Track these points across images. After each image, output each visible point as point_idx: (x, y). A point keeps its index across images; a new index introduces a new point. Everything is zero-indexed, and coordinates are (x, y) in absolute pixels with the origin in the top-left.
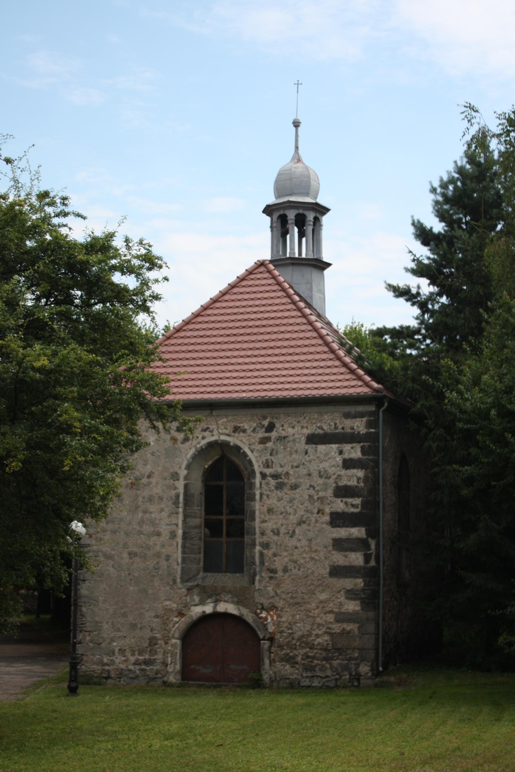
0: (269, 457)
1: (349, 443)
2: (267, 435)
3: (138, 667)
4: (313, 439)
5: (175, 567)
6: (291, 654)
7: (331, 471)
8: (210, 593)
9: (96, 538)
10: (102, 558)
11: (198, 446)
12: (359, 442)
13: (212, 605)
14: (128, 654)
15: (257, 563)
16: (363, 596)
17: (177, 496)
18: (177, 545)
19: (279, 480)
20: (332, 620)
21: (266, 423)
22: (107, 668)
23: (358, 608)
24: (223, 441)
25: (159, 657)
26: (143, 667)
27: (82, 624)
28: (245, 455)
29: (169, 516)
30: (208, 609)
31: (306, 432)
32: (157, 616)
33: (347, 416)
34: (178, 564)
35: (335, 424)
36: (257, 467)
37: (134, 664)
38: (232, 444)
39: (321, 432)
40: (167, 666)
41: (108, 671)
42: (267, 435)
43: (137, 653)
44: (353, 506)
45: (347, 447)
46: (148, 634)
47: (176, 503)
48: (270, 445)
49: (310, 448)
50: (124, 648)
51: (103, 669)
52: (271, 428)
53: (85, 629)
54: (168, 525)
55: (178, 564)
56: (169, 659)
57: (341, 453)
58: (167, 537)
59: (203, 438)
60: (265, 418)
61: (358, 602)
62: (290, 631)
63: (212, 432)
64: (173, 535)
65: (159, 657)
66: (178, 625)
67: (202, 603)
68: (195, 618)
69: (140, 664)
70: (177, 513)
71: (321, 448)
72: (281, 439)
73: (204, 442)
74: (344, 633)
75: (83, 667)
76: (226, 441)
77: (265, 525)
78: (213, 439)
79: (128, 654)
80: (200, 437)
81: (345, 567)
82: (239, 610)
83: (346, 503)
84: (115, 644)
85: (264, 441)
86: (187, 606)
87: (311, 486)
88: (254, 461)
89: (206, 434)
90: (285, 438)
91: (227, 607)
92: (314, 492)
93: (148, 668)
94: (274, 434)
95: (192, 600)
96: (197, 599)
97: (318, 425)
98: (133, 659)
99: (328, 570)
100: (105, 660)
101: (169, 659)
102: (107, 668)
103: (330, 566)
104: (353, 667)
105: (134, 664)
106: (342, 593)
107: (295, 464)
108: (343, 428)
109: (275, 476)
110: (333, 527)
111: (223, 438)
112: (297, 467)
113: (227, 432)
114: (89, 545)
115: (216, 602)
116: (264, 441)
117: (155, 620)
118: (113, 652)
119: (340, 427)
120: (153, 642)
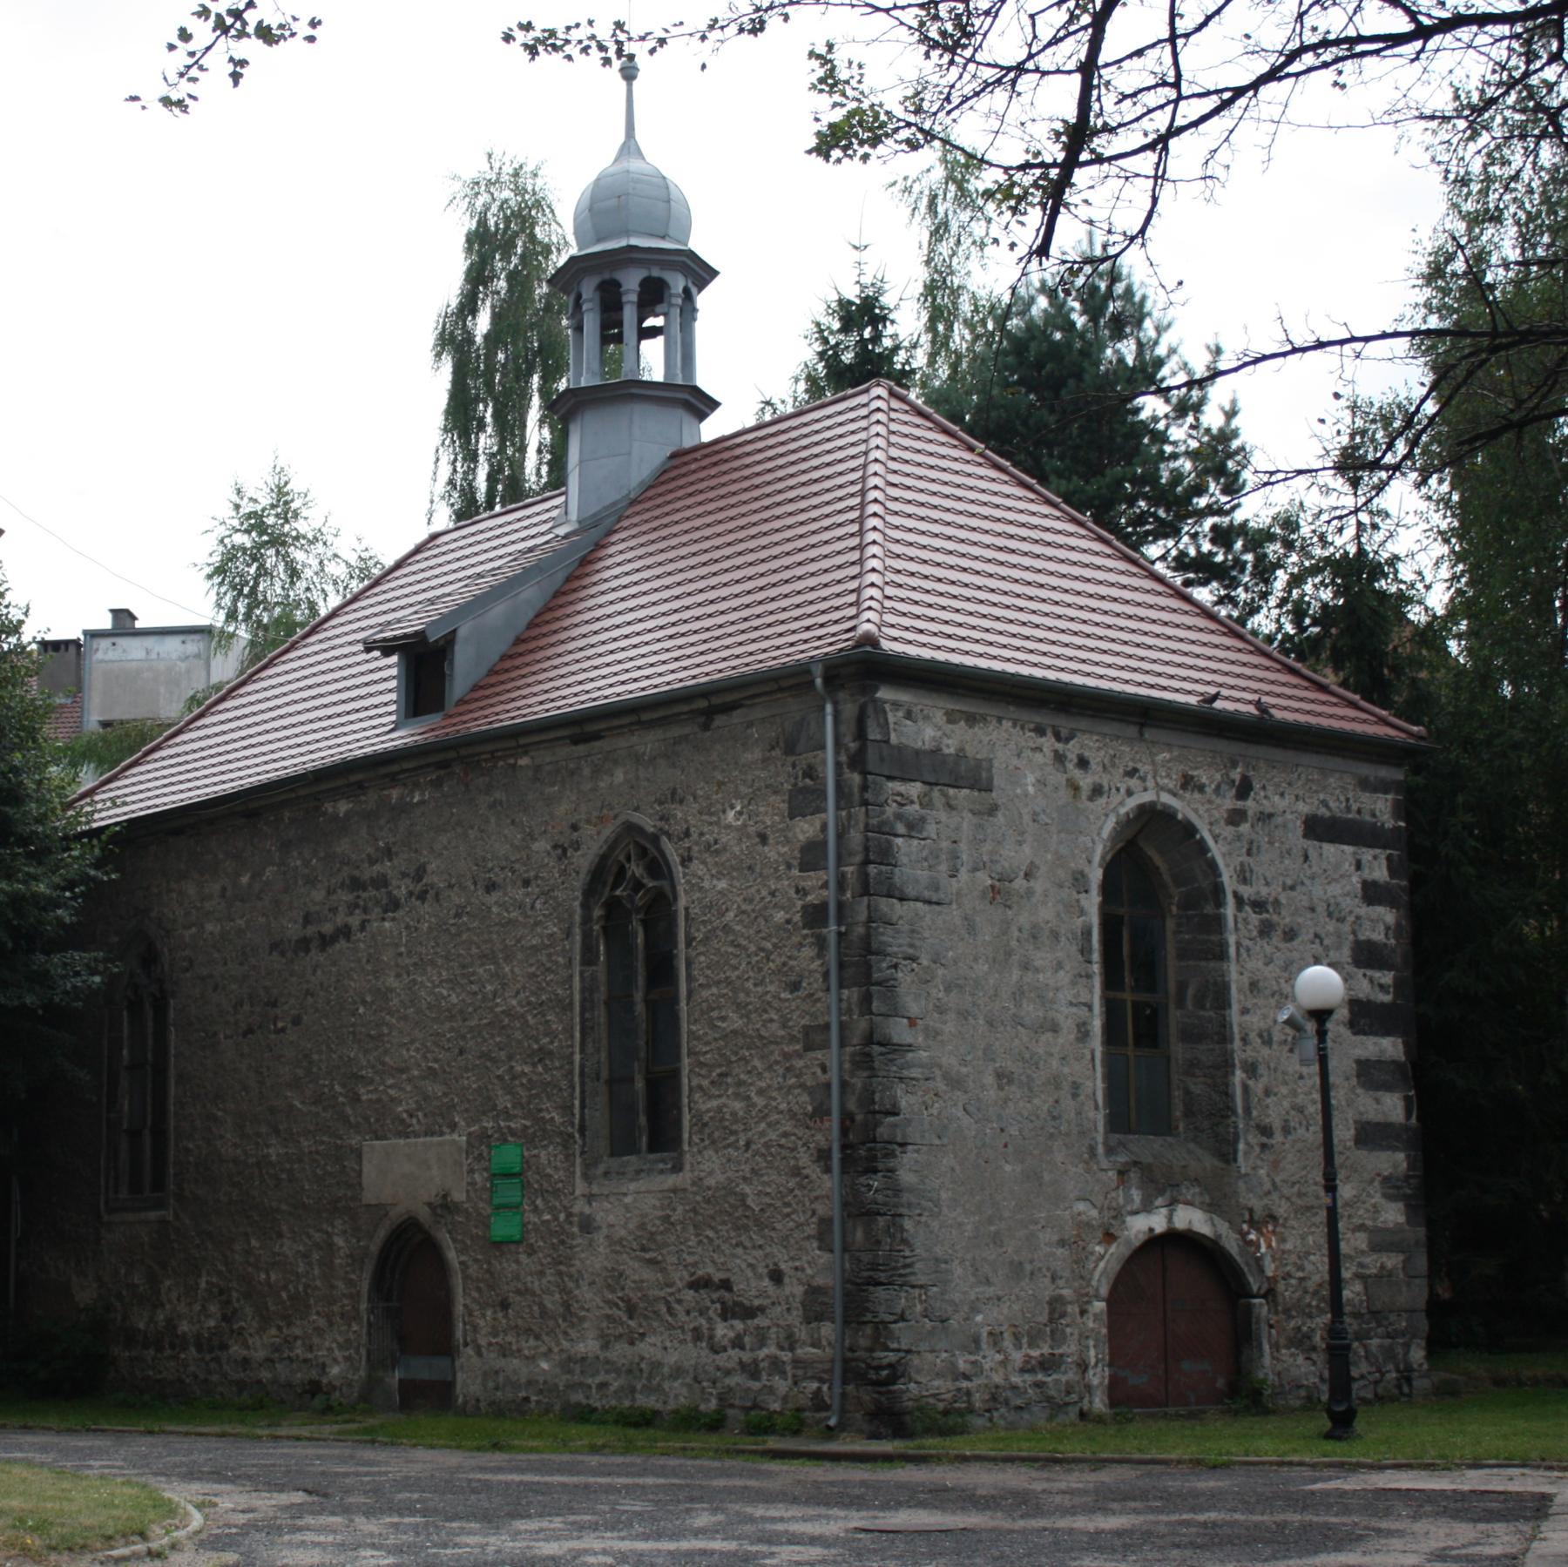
0: (1244, 858)
1: (1370, 846)
2: (1240, 804)
3: (1029, 1378)
4: (1320, 829)
5: (1091, 1114)
6: (1305, 1329)
7: (1347, 903)
8: (1161, 1185)
9: (926, 1028)
10: (941, 1086)
11: (1123, 811)
12: (1384, 847)
13: (1164, 1211)
14: (1008, 1343)
15: (1240, 1111)
16: (1409, 1191)
17: (1087, 933)
18: (1093, 1059)
19: (1265, 916)
20: (1364, 1246)
21: (1236, 775)
22: (965, 1384)
23: (1401, 1219)
24: (1164, 805)
25: (1070, 1348)
26: (1040, 1377)
27: (906, 1266)
28: (1202, 847)
29: (1073, 983)
30: (1157, 1222)
31: (1304, 808)
32: (1062, 1243)
33: (1365, 785)
34: (1097, 1108)
35: (1348, 800)
36: (1228, 879)
37: (1023, 1371)
38: (1180, 816)
39: (1328, 814)
40: (1085, 1370)
41: (968, 1393)
42: (1240, 804)
43: (1025, 1340)
44: (1381, 986)
45: (1367, 854)
46: (1046, 1290)
47: (1085, 951)
48: (1245, 828)
49: (1311, 844)
50: (998, 1330)
51: (959, 1390)
52: (1244, 790)
53: (912, 1279)
54: (1071, 1004)
55: (1097, 1108)
56: (1092, 1353)
57: (1359, 866)
58: (1072, 1037)
59: (1130, 793)
60: (1234, 765)
61: (1401, 1205)
62: (1300, 1274)
63: (1143, 779)
64: (1083, 1033)
65: (1070, 1348)
66: (1106, 1262)
67: (1147, 1208)
68: (1137, 1244)
69: (1032, 1371)
70: (1089, 976)
71: (1329, 849)
72: (1265, 817)
73: (1132, 803)
74: (1384, 1275)
75: (912, 1385)
76: (1170, 807)
77: (1247, 1018)
78: (1147, 797)
79: (1008, 1343)
80: (1123, 791)
81: (1378, 1124)
82: (1214, 1225)
83: (1371, 981)
84: (979, 1318)
85: (1236, 817)
86: (1119, 1215)
87: (1317, 936)
88: (1220, 862)
89: (1134, 783)
90: (1270, 816)
91: (1190, 1218)
92: (1320, 949)
93: (1049, 1379)
94: (1250, 804)
95: (1129, 1200)
96: (1136, 1195)
97: (1322, 796)
98: (1017, 1357)
99: (1352, 1132)
100: (962, 1365)
101: (1092, 1353)
102: (965, 1384)
103: (1355, 1122)
104: (1400, 1350)
105: (1023, 1371)
106: (1376, 1184)
107: (1289, 882)
108: (1359, 812)
109: (1259, 905)
110: (1355, 1034)
111: (1166, 798)
112: (1292, 888)
113: (1171, 786)
114: (910, 1048)
115: (1172, 1204)
116: (1236, 817)
117: (1060, 1251)
118: (976, 1341)
119: (1355, 807)
120: (1056, 1306)
